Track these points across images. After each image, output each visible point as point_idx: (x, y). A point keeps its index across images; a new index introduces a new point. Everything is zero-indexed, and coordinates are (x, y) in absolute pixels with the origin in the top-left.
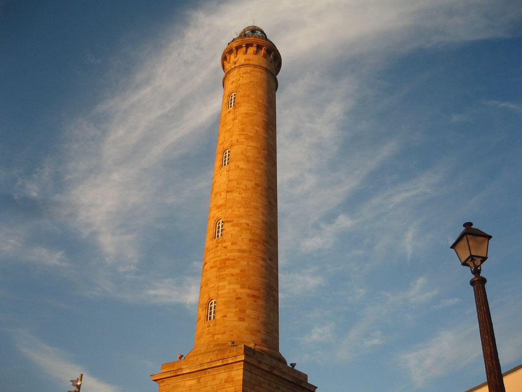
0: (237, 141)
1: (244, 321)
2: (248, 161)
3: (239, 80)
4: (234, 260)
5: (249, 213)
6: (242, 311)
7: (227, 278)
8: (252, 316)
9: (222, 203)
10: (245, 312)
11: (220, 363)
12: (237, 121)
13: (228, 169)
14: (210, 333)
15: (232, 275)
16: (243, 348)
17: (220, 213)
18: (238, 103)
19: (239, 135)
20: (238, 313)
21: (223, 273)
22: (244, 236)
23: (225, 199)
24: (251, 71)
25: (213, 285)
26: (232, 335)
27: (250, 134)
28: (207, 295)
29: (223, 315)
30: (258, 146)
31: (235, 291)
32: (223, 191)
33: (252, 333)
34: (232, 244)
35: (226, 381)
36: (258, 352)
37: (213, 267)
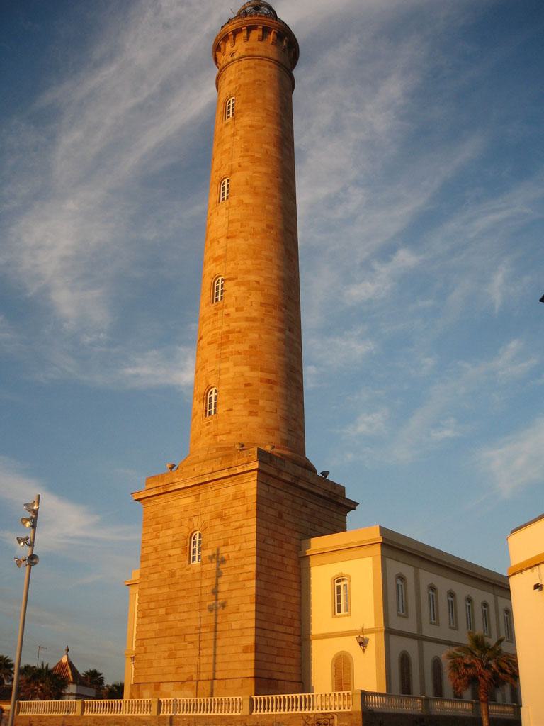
0: (240, 166)
1: (257, 415)
2: (255, 193)
3: (239, 78)
4: (239, 332)
5: (259, 266)
6: (254, 402)
7: (231, 357)
8: (268, 409)
9: (221, 253)
10: (257, 404)
11: (225, 474)
12: (238, 138)
13: (228, 206)
14: (212, 432)
15: (239, 353)
16: (256, 452)
17: (218, 267)
18: (239, 112)
19: (240, 157)
20: (248, 404)
21: (225, 351)
22: (252, 299)
23: (225, 248)
24: (255, 64)
25: (212, 368)
26: (241, 435)
27: (257, 155)
28: (204, 382)
29: (227, 408)
30: (270, 171)
31: (243, 376)
32: (222, 237)
33: (268, 432)
34: (237, 310)
36: (277, 457)
37: (212, 343)
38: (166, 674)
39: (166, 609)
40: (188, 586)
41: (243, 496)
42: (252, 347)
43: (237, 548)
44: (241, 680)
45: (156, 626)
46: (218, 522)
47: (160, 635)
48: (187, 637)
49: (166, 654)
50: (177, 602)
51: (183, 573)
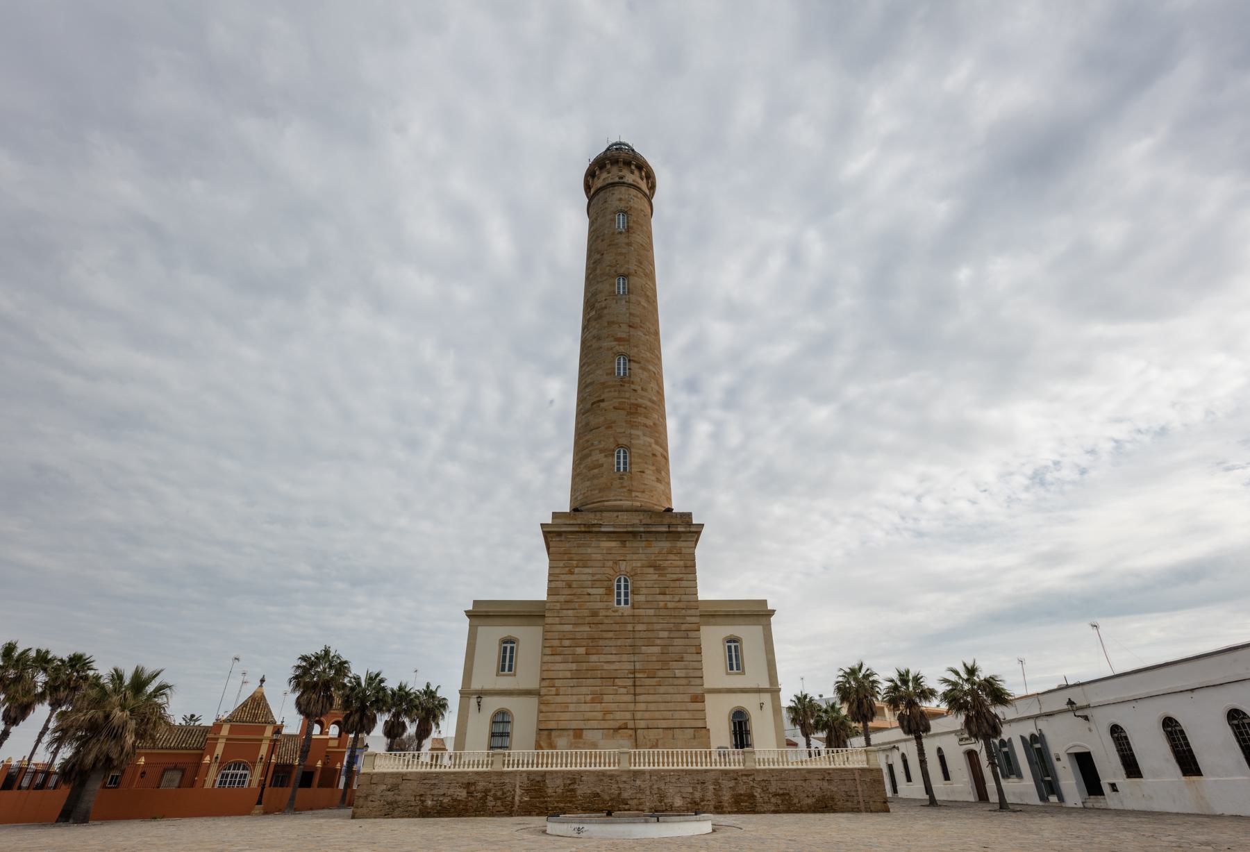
14: (625, 487)
25: (623, 430)
26: (652, 496)
29: (641, 470)
35: (670, 553)
38: (589, 720)
39: (587, 649)
40: (617, 627)
41: (679, 551)
43: (677, 598)
44: (693, 730)
45: (574, 666)
46: (651, 570)
47: (577, 676)
48: (616, 680)
49: (589, 698)
50: (601, 642)
51: (608, 614)
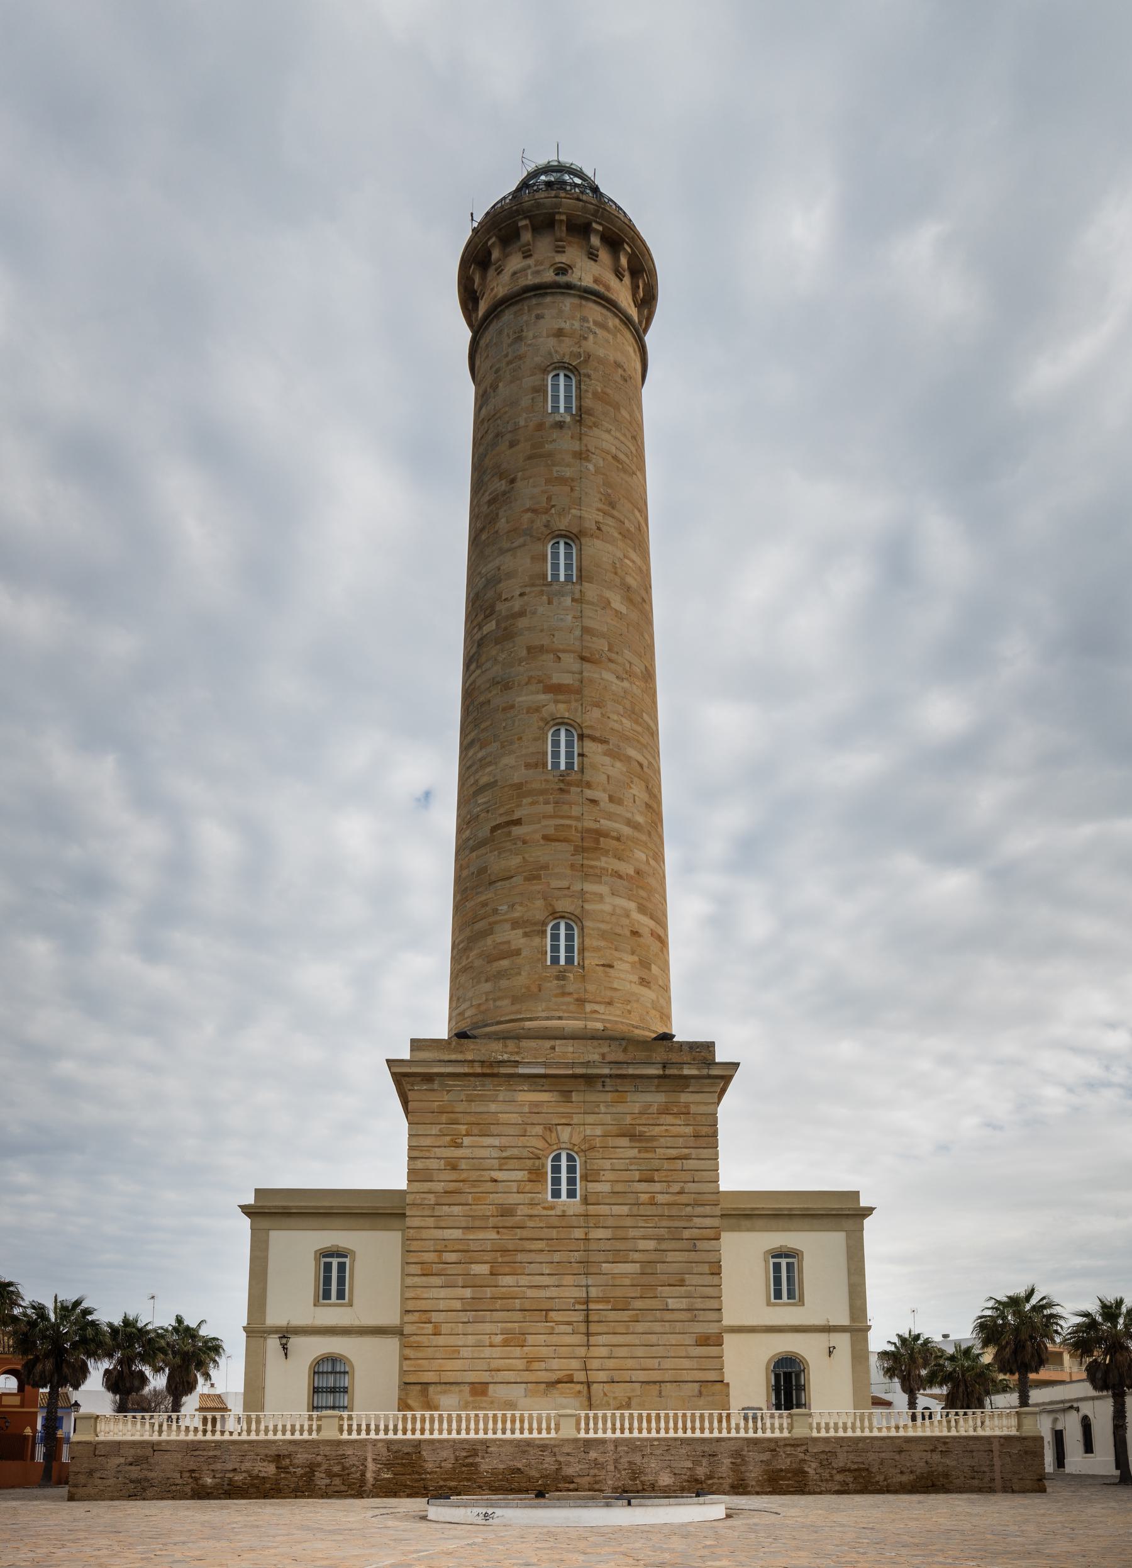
1: (650, 988)
7: (604, 878)
20: (638, 966)
25: (565, 884)
26: (630, 1012)
42: (638, 873)
